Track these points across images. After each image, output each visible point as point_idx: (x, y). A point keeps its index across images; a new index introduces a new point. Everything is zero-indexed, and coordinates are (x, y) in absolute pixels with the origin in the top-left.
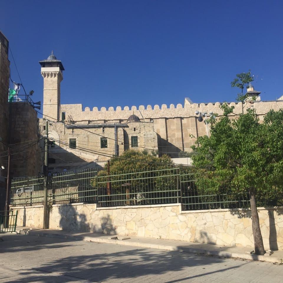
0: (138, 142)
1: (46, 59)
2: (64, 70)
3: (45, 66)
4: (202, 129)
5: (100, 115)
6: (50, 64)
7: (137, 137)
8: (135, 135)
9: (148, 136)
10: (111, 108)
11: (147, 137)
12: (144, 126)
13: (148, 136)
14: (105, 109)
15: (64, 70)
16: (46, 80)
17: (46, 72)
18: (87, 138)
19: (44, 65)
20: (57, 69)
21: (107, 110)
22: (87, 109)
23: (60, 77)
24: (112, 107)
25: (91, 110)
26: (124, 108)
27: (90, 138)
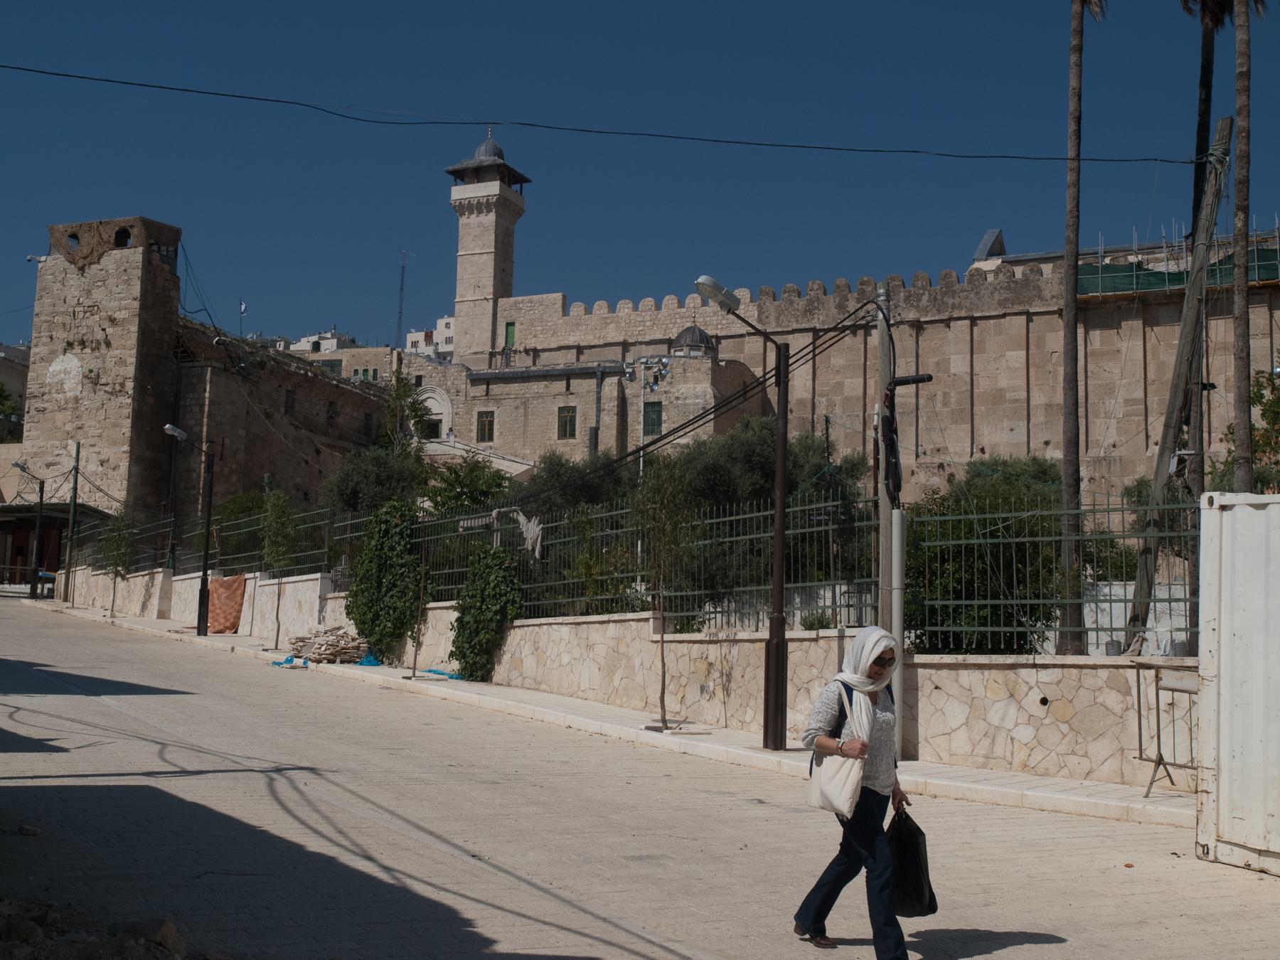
0: (663, 419)
1: (472, 156)
2: (528, 181)
3: (466, 180)
4: (938, 364)
5: (612, 326)
6: (477, 174)
7: (659, 404)
8: (653, 398)
9: (687, 401)
10: (648, 302)
11: (685, 405)
12: (685, 370)
13: (687, 401)
14: (631, 305)
15: (528, 181)
16: (466, 224)
17: (472, 200)
18: (521, 411)
19: (462, 176)
20: (492, 188)
21: (636, 308)
22: (577, 309)
23: (506, 209)
24: (651, 299)
25: (589, 311)
26: (687, 302)
27: (530, 410)
